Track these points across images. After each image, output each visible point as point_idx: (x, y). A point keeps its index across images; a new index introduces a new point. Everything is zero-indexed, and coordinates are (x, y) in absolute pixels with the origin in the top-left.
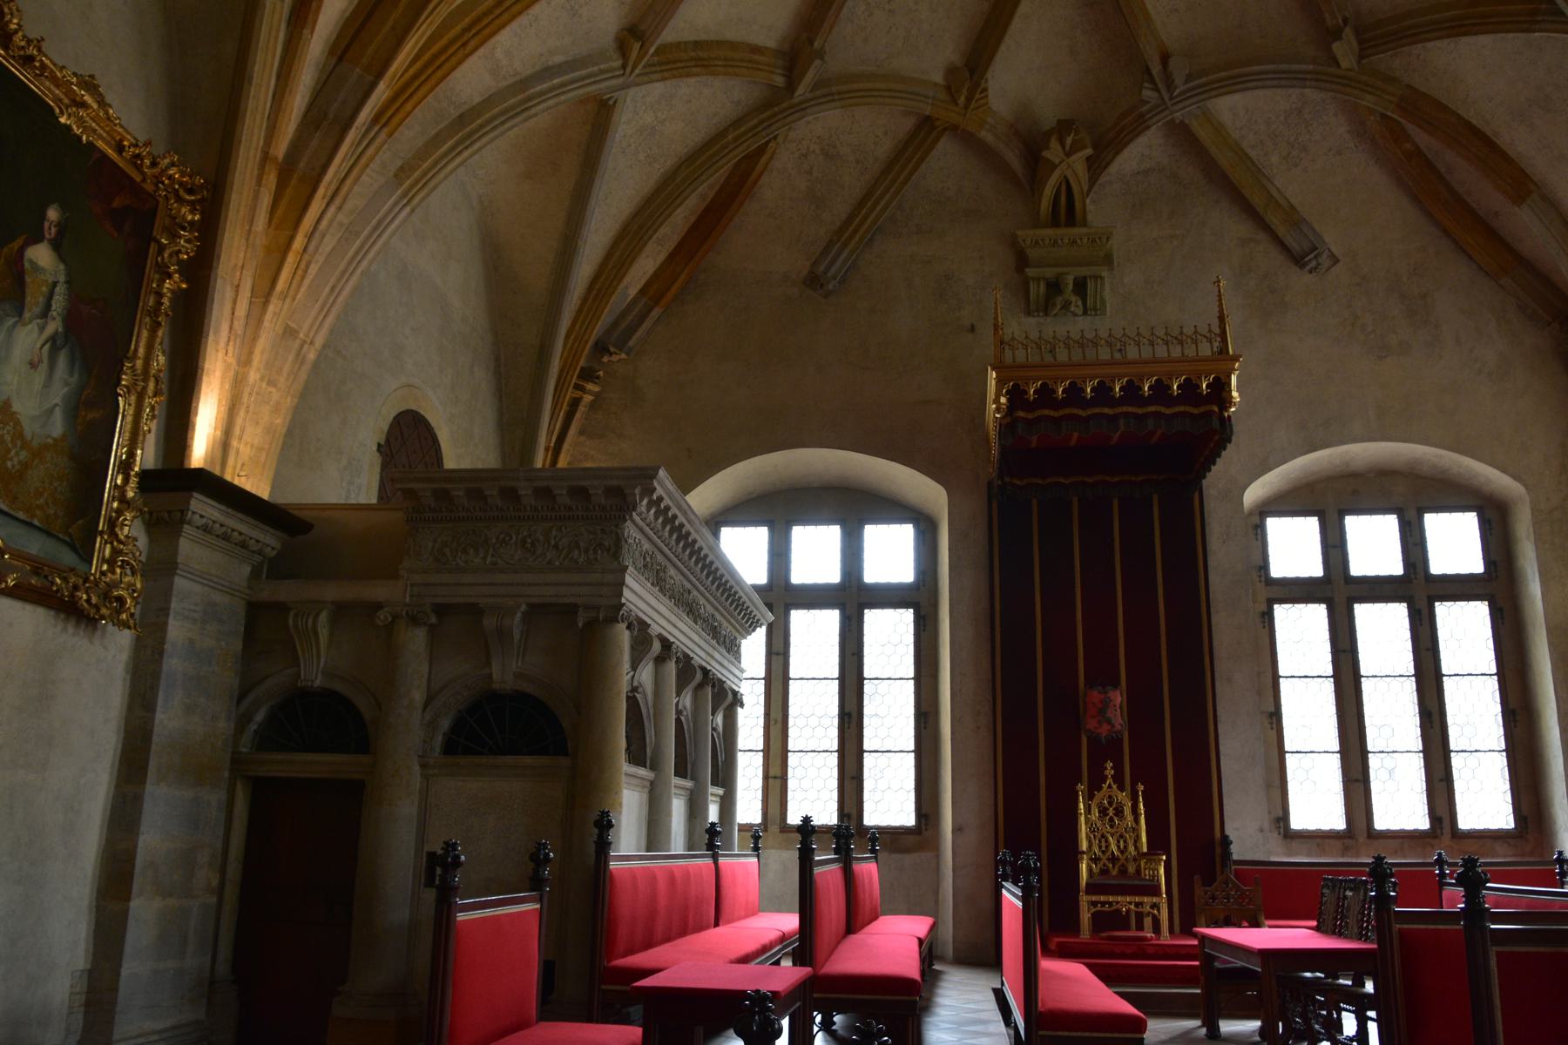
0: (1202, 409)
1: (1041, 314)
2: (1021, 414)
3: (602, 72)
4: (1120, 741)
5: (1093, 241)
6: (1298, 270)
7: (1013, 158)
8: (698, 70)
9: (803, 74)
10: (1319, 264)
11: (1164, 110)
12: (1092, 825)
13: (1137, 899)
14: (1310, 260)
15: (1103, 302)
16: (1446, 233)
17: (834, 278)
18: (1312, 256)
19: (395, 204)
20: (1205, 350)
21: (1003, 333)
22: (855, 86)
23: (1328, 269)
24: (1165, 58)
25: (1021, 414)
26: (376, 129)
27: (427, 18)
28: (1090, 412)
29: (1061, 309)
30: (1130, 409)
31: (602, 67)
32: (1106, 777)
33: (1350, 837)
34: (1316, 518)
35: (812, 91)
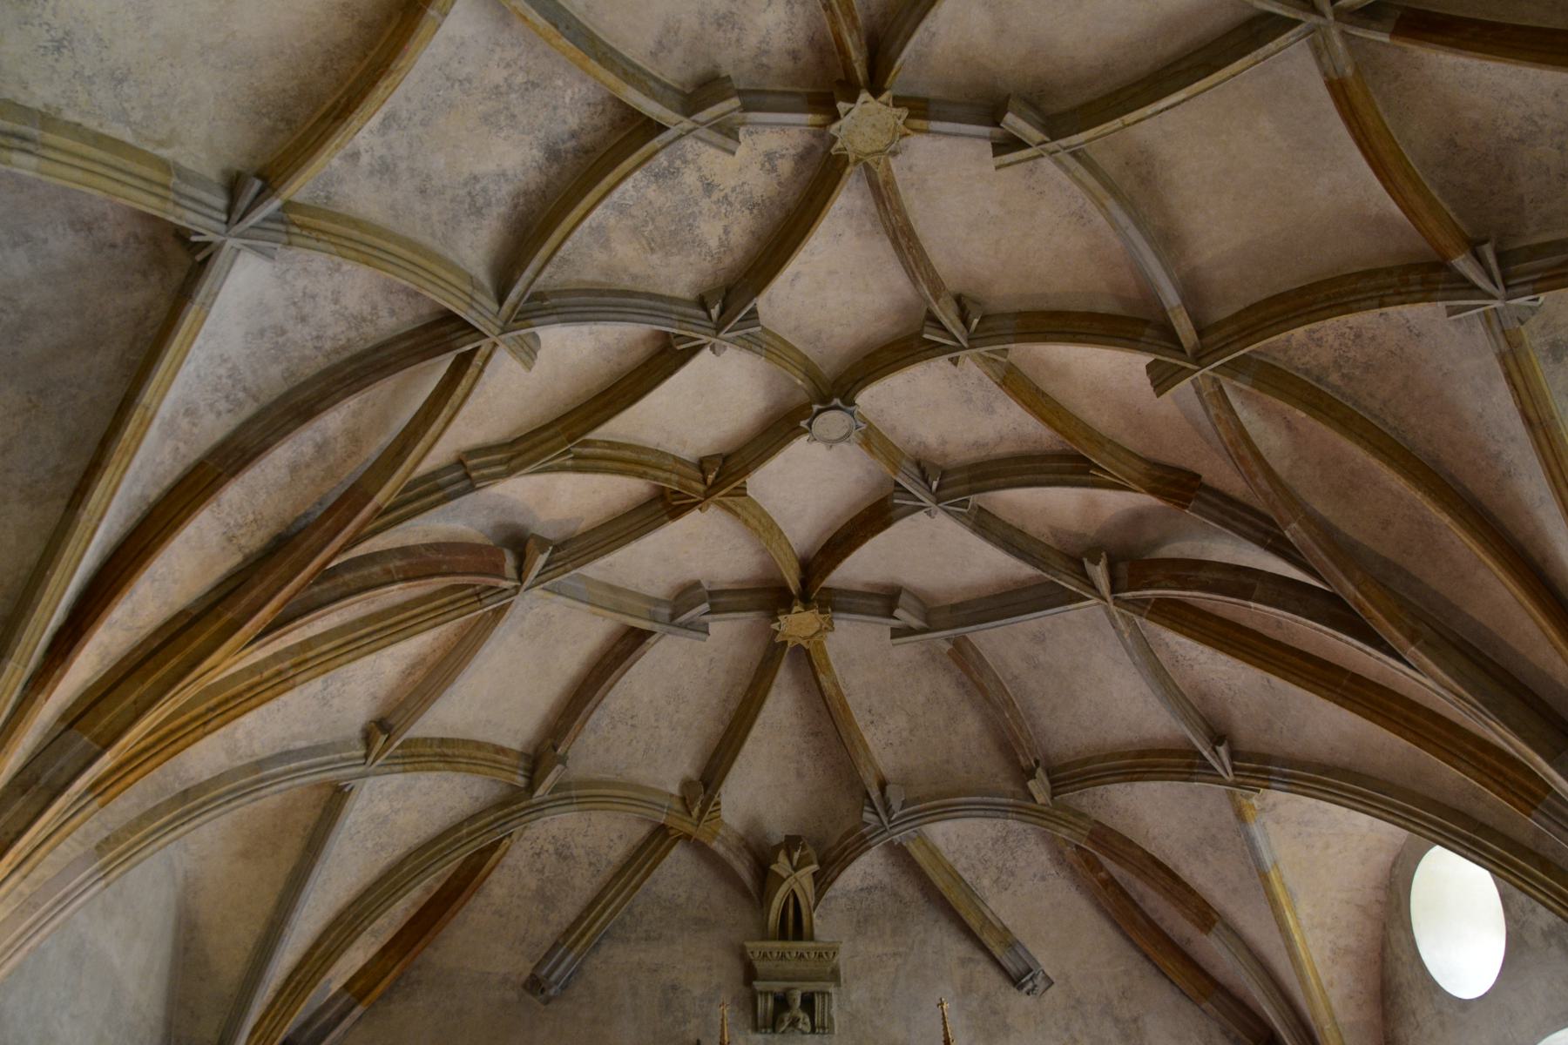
1: (769, 1031)
3: (343, 760)
5: (820, 956)
7: (743, 868)
8: (441, 765)
9: (544, 777)
14: (1027, 981)
15: (831, 1019)
16: (1147, 957)
17: (556, 983)
18: (1028, 977)
19: (90, 876)
22: (594, 792)
23: (1046, 989)
24: (883, 785)
26: (90, 797)
27: (172, 697)
29: (789, 1026)
31: (345, 755)
35: (551, 792)
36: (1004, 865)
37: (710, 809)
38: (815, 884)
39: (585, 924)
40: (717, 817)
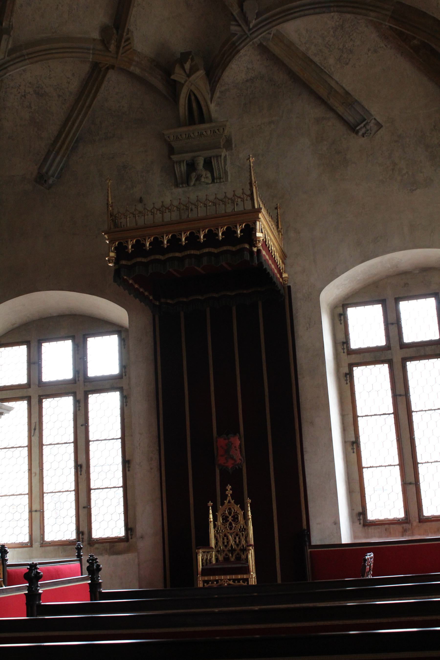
0: (238, 247)
1: (184, 185)
2: (124, 262)
4: (241, 470)
5: (214, 132)
6: (355, 136)
10: (368, 130)
11: (245, 39)
12: (218, 529)
13: (234, 577)
14: (361, 128)
15: (226, 173)
17: (53, 176)
18: (362, 125)
20: (239, 208)
21: (113, 209)
22: (37, 48)
25: (124, 262)
28: (167, 256)
30: (192, 252)
32: (227, 495)
33: (407, 523)
34: (380, 305)
36: (344, 46)
37: (123, 44)
38: (210, 84)
39: (63, 135)
40: (129, 50)
